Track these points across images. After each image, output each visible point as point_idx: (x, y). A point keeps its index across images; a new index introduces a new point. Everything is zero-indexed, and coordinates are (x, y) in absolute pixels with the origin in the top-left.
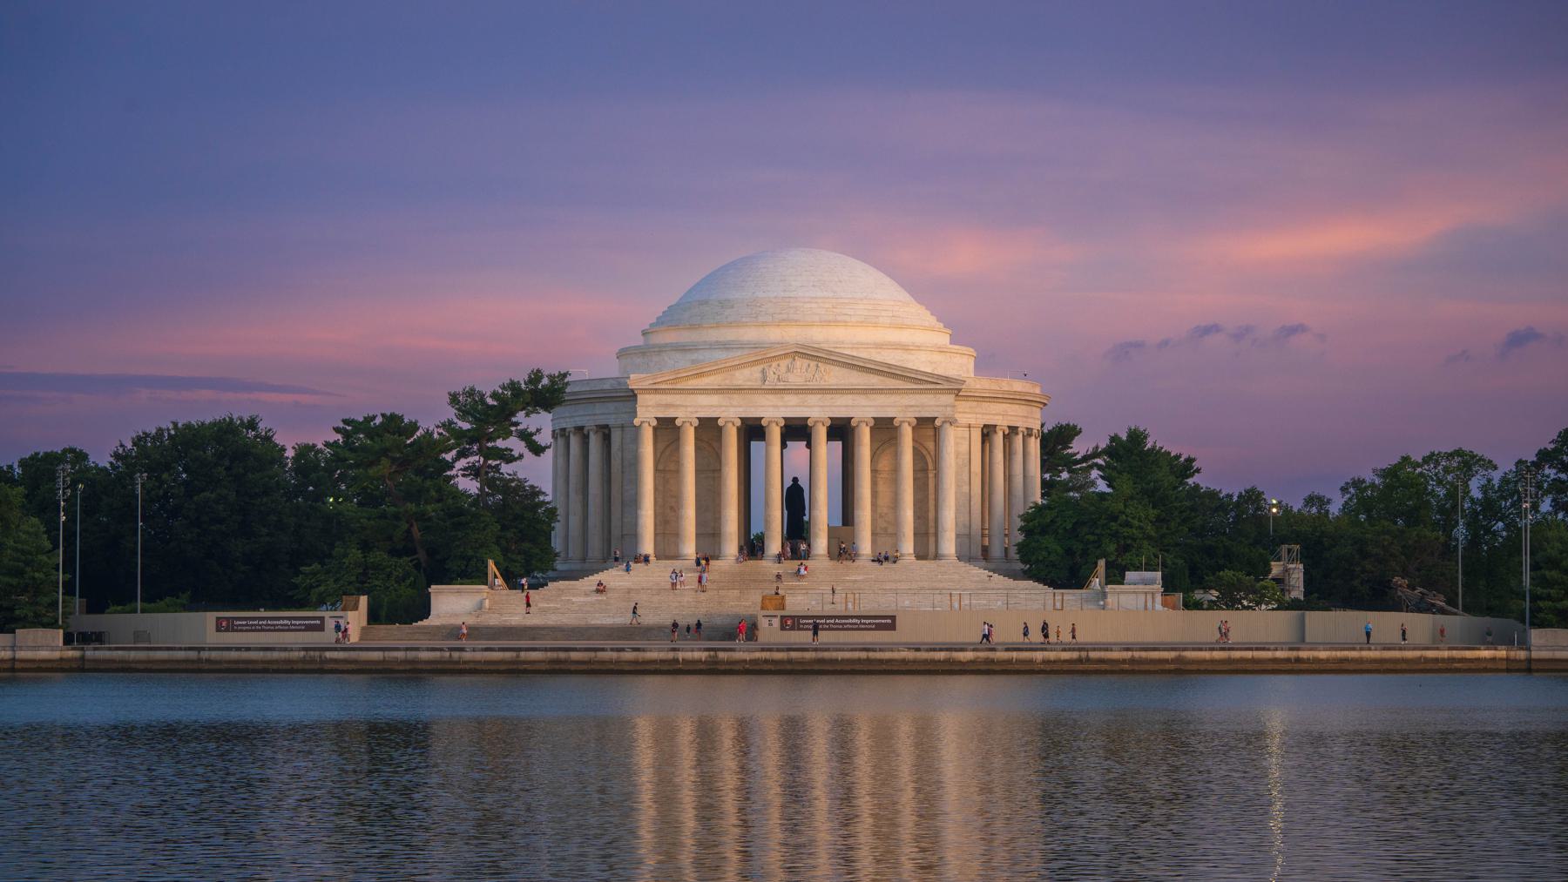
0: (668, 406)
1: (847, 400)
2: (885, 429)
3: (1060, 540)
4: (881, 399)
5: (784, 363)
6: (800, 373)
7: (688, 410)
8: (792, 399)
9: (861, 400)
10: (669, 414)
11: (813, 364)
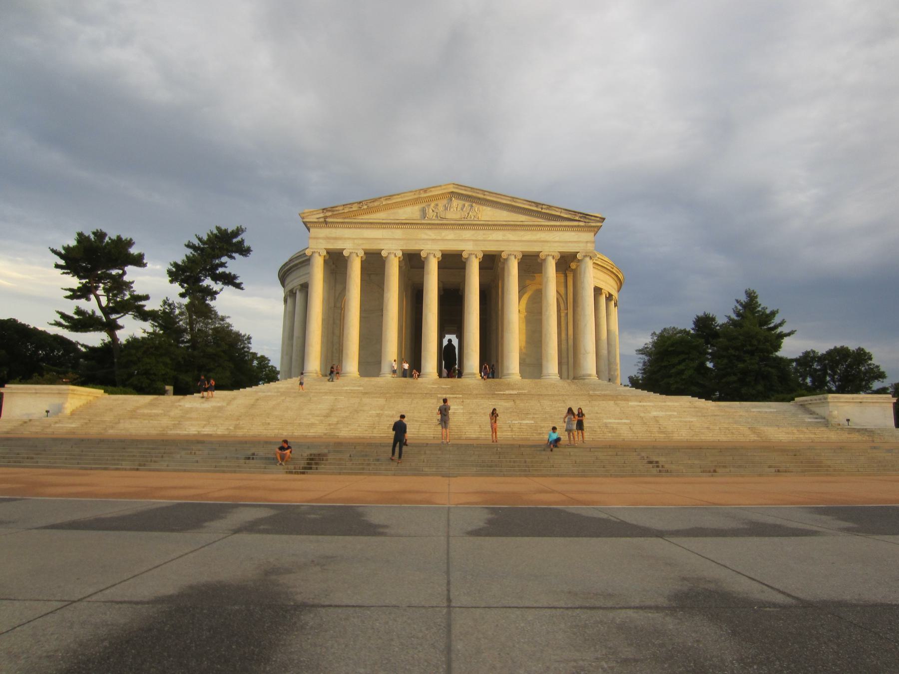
0: (335, 239)
2: (531, 265)
3: (675, 365)
4: (529, 236)
5: (442, 203)
6: (456, 210)
7: (353, 242)
8: (449, 234)
9: (511, 236)
10: (338, 245)
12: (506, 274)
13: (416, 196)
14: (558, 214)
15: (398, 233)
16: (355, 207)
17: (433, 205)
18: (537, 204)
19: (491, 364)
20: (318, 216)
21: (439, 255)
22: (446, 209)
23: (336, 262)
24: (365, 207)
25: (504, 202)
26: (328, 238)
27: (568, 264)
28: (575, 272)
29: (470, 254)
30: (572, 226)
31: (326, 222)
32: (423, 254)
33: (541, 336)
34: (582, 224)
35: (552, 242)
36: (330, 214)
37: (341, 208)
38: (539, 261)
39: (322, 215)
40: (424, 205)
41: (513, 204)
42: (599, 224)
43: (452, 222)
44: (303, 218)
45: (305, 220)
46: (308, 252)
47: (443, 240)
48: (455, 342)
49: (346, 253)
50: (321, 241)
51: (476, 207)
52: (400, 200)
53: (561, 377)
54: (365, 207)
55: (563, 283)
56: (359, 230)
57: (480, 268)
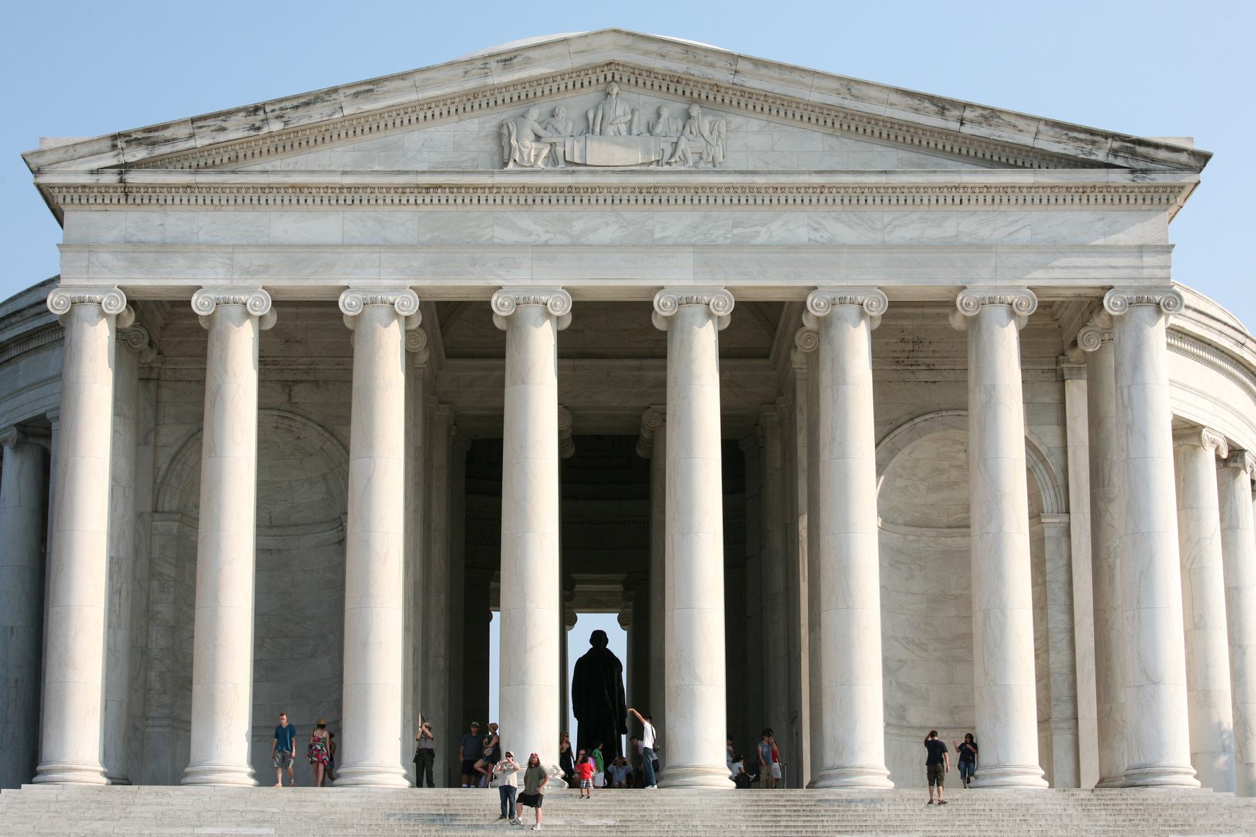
0: (165, 248)
1: (792, 226)
4: (911, 227)
8: (602, 226)
9: (840, 228)
11: (672, 108)
12: (825, 378)
13: (471, 84)
14: (1026, 140)
15: (403, 222)
16: (236, 131)
17: (534, 113)
18: (942, 105)
19: (771, 732)
20: (95, 165)
21: (563, 308)
22: (588, 129)
23: (164, 343)
24: (276, 126)
25: (815, 97)
26: (131, 248)
27: (1067, 338)
28: (1092, 369)
29: (684, 302)
30: (1083, 189)
31: (127, 191)
32: (501, 306)
33: (967, 618)
34: (1119, 178)
35: (1006, 254)
36: (140, 154)
37: (184, 131)
38: (956, 323)
39: (109, 160)
40: (506, 114)
41: (850, 104)
42: (1188, 178)
43: (614, 180)
44: (37, 172)
45: (44, 179)
46: (56, 302)
47: (576, 246)
48: (619, 644)
49: (200, 305)
50: (105, 257)
51: (704, 122)
52: (413, 97)
53: (1049, 777)
54: (276, 126)
55: (1046, 404)
56: (250, 216)
57: (562, 355)
